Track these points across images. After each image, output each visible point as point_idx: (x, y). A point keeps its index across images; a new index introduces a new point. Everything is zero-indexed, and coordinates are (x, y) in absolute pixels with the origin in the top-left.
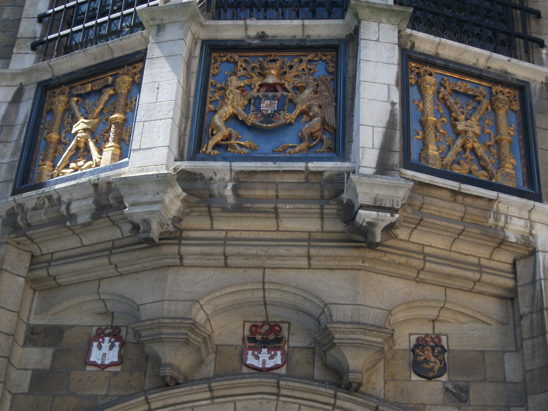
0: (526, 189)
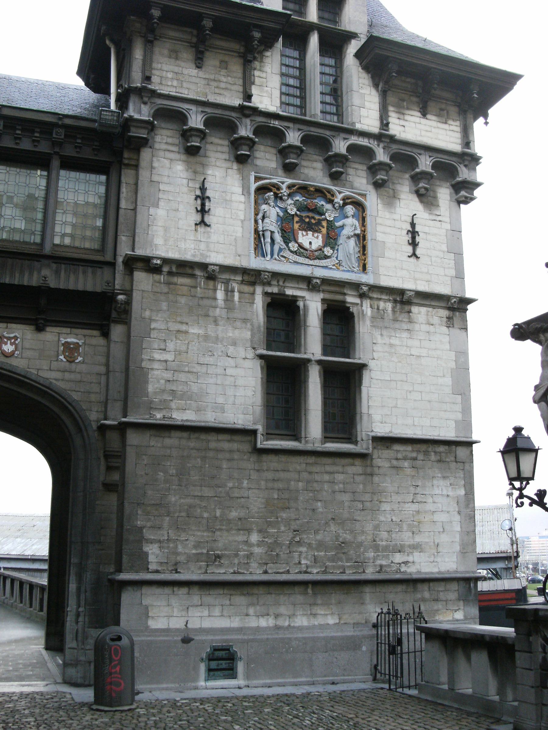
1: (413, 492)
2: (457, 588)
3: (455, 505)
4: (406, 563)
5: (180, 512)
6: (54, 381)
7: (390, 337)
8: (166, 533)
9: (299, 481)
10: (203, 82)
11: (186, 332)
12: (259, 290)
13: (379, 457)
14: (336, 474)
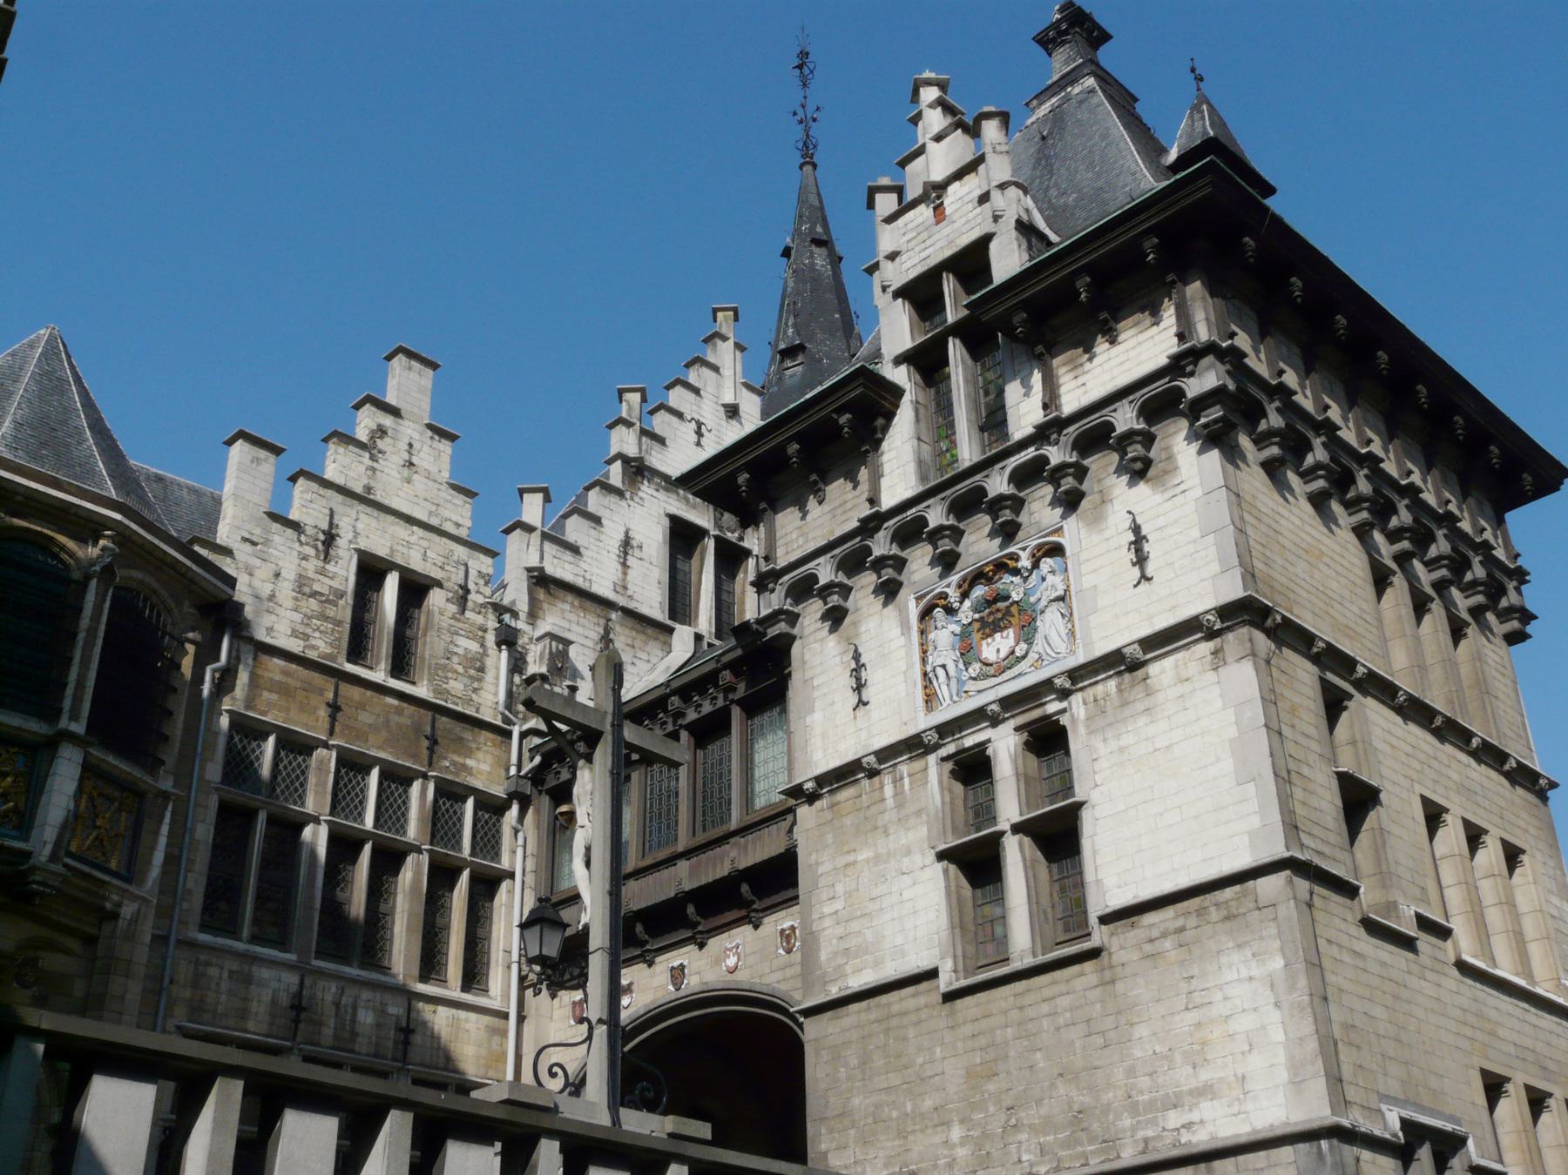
0: (124, 872)
1: (1185, 991)
2: (1292, 1159)
3: (1268, 992)
4: (1188, 1126)
5: (866, 1118)
6: (776, 985)
7: (1118, 737)
8: (852, 1153)
9: (1007, 1027)
10: (829, 516)
11: (855, 862)
12: (932, 759)
13: (1122, 948)
14: (1058, 999)
